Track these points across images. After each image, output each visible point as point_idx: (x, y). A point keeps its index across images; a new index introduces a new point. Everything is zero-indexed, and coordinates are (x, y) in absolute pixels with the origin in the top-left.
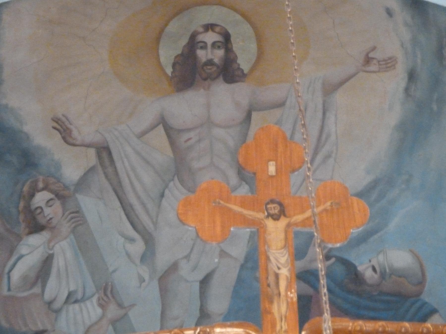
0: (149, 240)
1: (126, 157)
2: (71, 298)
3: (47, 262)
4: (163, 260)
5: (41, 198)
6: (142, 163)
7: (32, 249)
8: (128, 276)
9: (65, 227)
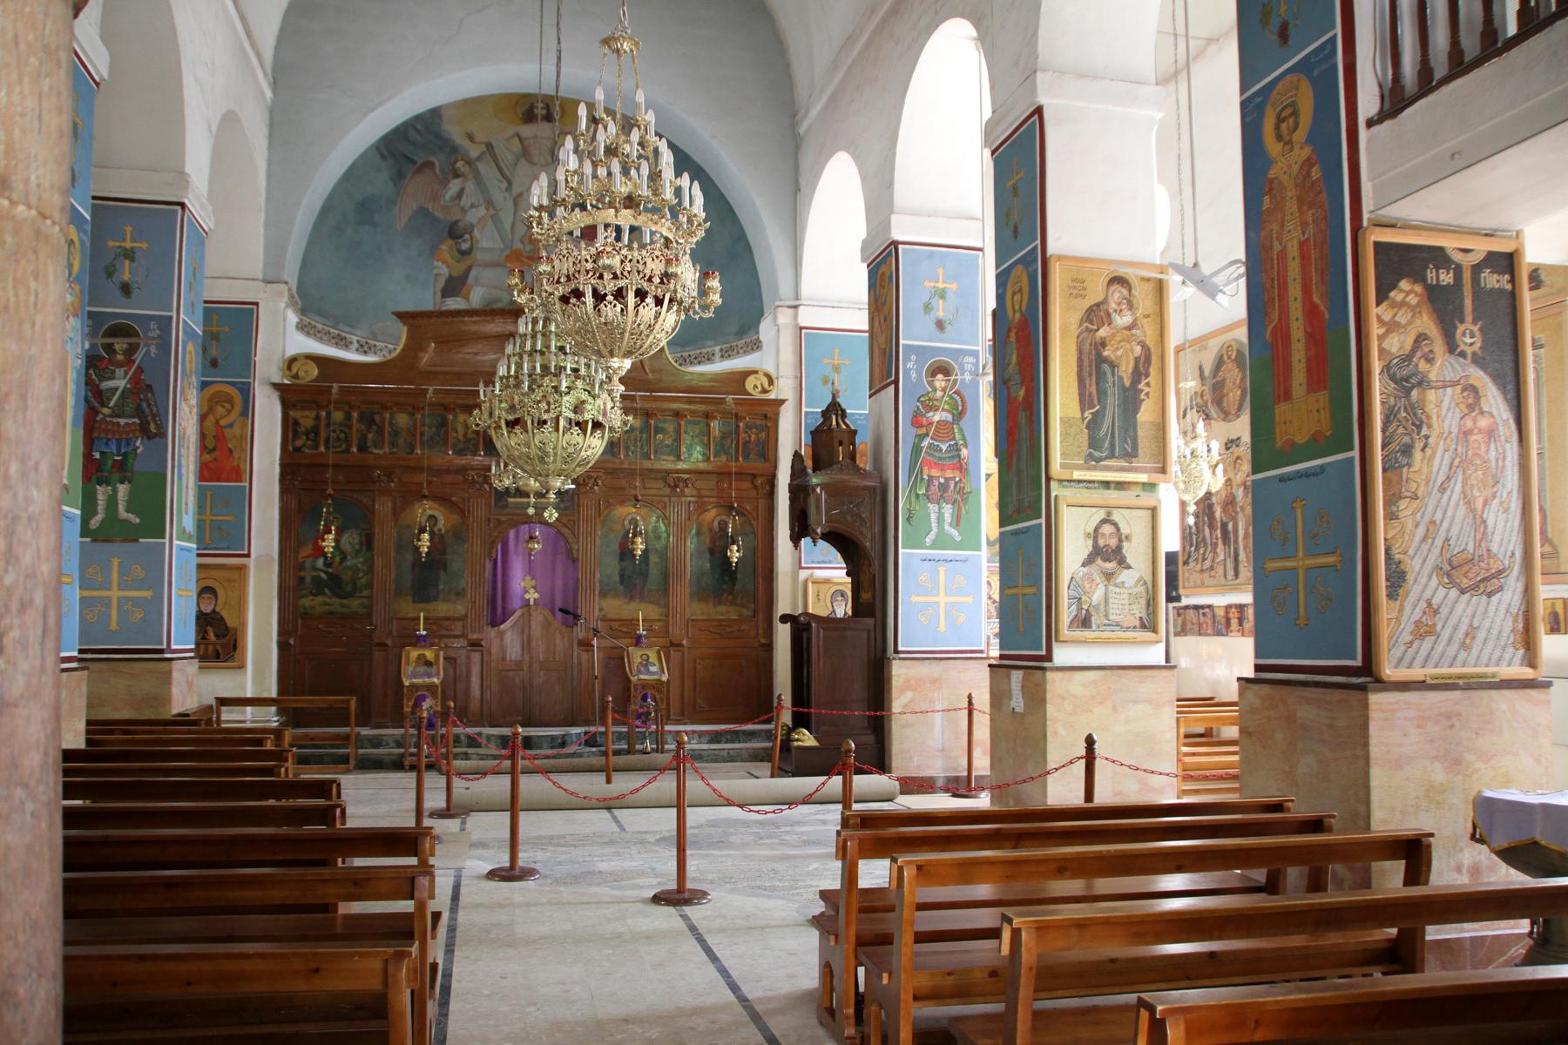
0: (509, 182)
1: (499, 148)
2: (473, 206)
3: (462, 191)
4: (515, 191)
5: (459, 164)
6: (506, 153)
7: (455, 185)
8: (498, 195)
9: (471, 176)
